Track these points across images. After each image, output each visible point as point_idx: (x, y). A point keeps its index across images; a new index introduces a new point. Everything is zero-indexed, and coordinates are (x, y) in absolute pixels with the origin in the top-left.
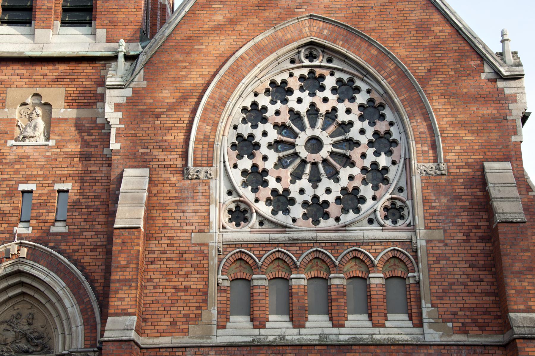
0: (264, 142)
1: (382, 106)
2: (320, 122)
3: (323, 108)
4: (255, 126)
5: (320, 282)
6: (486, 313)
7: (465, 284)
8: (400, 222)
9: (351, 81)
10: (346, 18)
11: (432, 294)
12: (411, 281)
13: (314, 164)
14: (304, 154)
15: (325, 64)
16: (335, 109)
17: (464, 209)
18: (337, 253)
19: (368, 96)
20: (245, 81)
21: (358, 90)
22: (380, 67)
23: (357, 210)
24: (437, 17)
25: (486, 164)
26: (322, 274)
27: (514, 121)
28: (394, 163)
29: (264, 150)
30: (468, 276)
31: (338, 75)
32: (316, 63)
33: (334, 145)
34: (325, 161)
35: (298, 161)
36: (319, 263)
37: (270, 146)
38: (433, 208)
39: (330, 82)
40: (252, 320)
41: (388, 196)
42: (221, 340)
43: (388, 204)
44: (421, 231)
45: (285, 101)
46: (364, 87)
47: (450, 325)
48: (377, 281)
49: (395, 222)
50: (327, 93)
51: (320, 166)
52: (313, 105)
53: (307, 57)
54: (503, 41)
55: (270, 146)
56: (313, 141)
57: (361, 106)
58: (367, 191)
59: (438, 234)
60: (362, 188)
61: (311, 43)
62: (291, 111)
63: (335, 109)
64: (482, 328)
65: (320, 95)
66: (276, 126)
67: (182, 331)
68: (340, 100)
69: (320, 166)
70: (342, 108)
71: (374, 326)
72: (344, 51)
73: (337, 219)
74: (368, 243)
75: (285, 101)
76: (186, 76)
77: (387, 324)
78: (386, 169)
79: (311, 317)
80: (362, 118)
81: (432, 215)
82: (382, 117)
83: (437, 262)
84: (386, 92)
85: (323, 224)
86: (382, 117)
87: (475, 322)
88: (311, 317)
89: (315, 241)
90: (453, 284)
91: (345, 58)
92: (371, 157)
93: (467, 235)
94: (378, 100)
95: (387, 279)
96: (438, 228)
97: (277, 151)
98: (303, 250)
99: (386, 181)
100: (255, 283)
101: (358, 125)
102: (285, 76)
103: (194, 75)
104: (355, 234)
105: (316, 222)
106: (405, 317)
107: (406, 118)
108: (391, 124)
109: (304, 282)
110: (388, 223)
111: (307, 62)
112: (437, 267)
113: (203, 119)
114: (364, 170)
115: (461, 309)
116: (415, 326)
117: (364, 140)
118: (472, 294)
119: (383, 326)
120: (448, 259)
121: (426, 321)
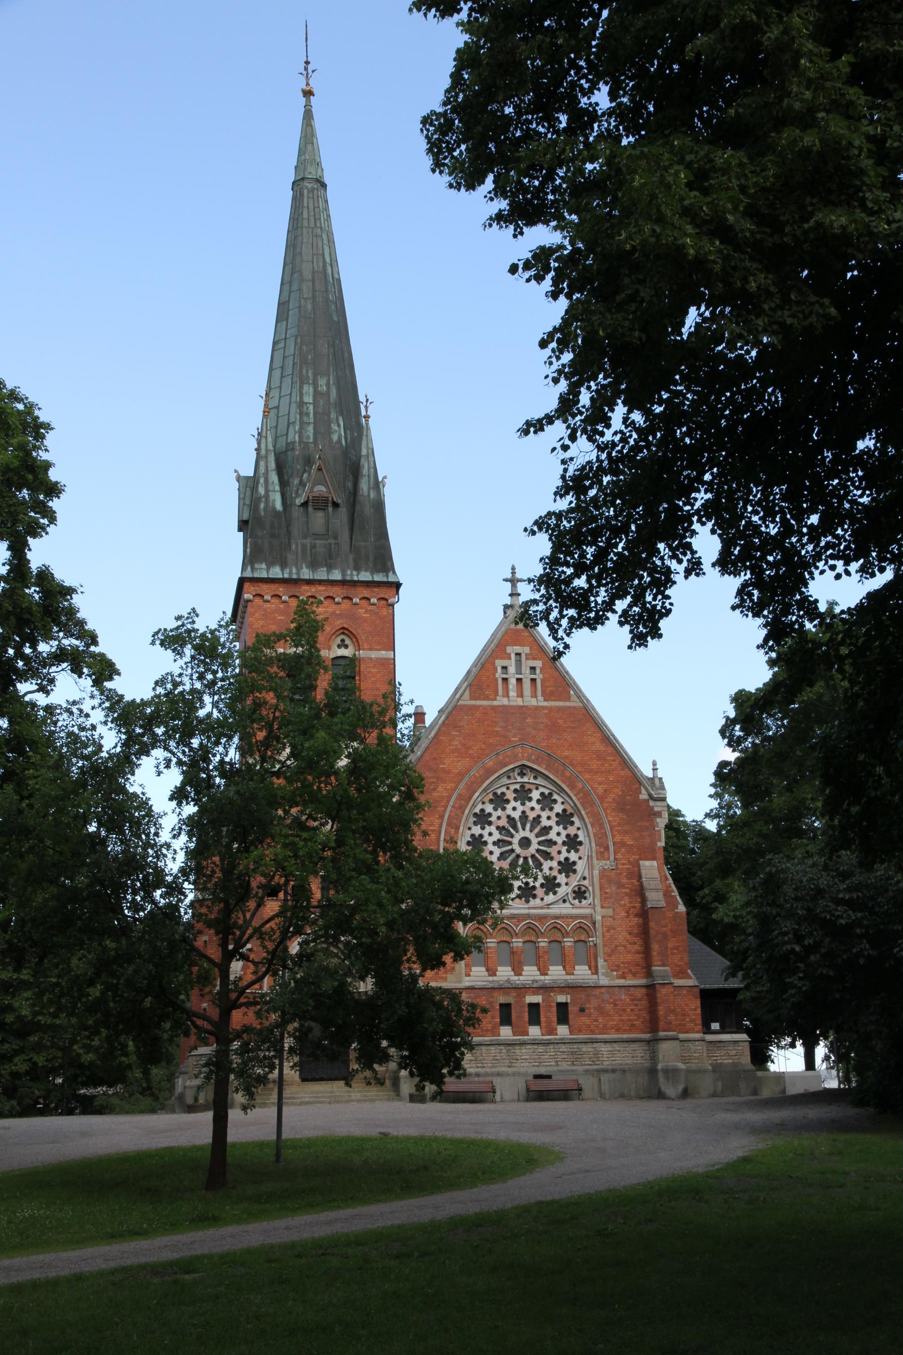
0: (490, 840)
1: (572, 815)
2: (528, 826)
3: (532, 815)
4: (483, 828)
5: (531, 944)
6: (637, 965)
7: (625, 946)
8: (584, 902)
9: (550, 794)
10: (547, 746)
11: (604, 953)
12: (591, 944)
13: (526, 858)
14: (518, 850)
15: (532, 781)
16: (539, 816)
17: (626, 894)
18: (543, 924)
19: (562, 807)
20: (477, 794)
21: (555, 801)
22: (572, 786)
23: (555, 893)
24: (610, 750)
25: (641, 862)
26: (533, 939)
27: (659, 831)
28: (580, 858)
29: (490, 847)
30: (627, 941)
31: (542, 790)
32: (525, 779)
33: (539, 843)
34: (533, 856)
35: (513, 855)
36: (531, 931)
37: (494, 843)
38: (606, 893)
39: (536, 795)
40: (487, 970)
41: (576, 883)
42: (468, 984)
43: (576, 889)
44: (598, 909)
45: (504, 809)
46: (560, 800)
47: (615, 973)
48: (569, 944)
49: (580, 902)
50: (533, 804)
51: (530, 860)
52: (523, 812)
53: (519, 774)
54: (654, 770)
55: (494, 843)
56: (525, 841)
57: (558, 815)
58: (561, 879)
59: (610, 912)
60: (559, 876)
61: (523, 765)
62: (508, 817)
63: (539, 816)
64: (635, 975)
65: (529, 804)
66: (498, 828)
67: (442, 978)
68: (543, 809)
69: (530, 860)
70: (544, 815)
71: (567, 974)
72: (546, 773)
73: (542, 899)
74: (563, 918)
75: (504, 809)
76: (435, 789)
77: (575, 972)
78: (574, 863)
79: (525, 968)
80: (558, 824)
81: (606, 898)
82: (572, 823)
83: (608, 931)
84: (575, 805)
85: (532, 902)
86: (572, 823)
87: (630, 971)
88: (525, 968)
89: (528, 916)
90: (616, 946)
91: (546, 777)
92: (564, 854)
93: (627, 912)
94: (570, 811)
95: (575, 942)
96: (609, 907)
97: (499, 847)
98: (520, 921)
99: (575, 872)
100: (489, 945)
101: (556, 829)
102: (504, 789)
103: (440, 789)
104: (555, 910)
105: (527, 901)
106: (587, 967)
107: (589, 826)
108: (578, 829)
109: (520, 944)
110: (577, 901)
111: (519, 779)
112: (608, 935)
113: (448, 825)
114: (560, 863)
115: (623, 963)
116: (593, 974)
117: (559, 840)
118: (629, 952)
119: (573, 974)
120: (615, 929)
121: (600, 971)
